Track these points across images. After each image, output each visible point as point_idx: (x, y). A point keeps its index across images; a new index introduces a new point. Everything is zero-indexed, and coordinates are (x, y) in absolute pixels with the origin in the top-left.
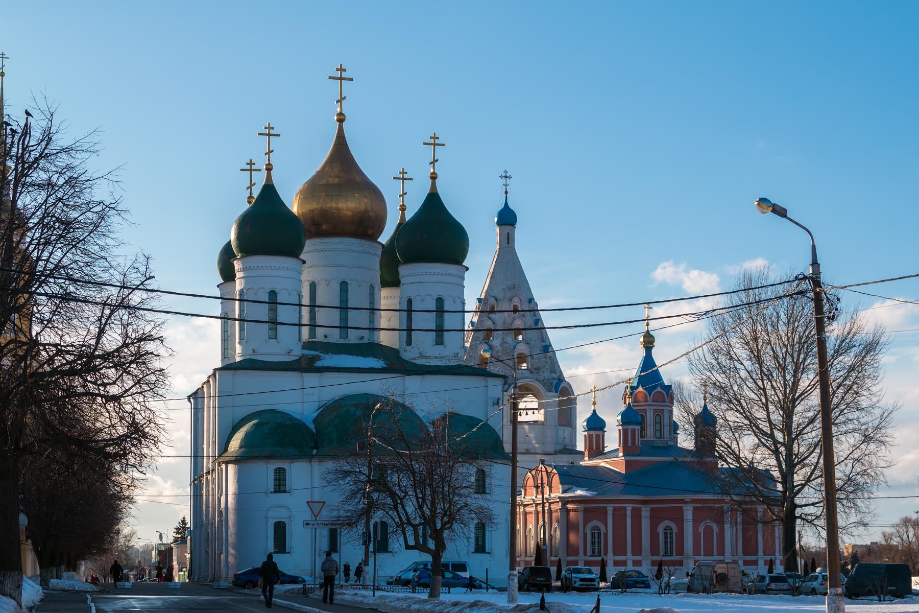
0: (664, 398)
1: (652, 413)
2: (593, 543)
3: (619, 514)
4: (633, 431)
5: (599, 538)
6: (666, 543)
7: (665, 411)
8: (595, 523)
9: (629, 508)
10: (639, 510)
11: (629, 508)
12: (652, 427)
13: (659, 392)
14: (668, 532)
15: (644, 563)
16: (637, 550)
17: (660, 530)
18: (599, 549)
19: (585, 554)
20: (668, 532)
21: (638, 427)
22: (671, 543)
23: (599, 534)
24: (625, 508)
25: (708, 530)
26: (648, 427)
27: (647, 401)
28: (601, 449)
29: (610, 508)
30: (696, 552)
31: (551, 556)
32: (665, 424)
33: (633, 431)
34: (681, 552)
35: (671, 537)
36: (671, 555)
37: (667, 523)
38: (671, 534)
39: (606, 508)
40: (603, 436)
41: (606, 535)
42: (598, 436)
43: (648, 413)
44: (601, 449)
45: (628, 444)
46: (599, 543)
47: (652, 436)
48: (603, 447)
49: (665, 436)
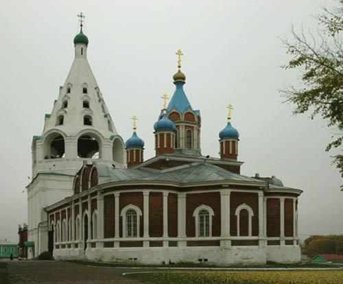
0: (194, 118)
2: (129, 226)
3: (156, 199)
4: (168, 135)
5: (135, 221)
6: (201, 225)
8: (131, 207)
9: (166, 193)
10: (176, 196)
11: (166, 193)
13: (189, 113)
14: (205, 216)
15: (179, 243)
16: (173, 232)
17: (196, 214)
18: (135, 230)
19: (121, 236)
20: (205, 216)
21: (172, 133)
22: (208, 225)
23: (135, 217)
24: (161, 194)
25: (244, 212)
26: (181, 140)
29: (146, 192)
30: (233, 233)
31: (92, 238)
33: (168, 135)
34: (217, 232)
35: (208, 220)
37: (203, 207)
38: (208, 217)
39: (142, 193)
40: (142, 152)
41: (142, 218)
42: (137, 151)
43: (180, 129)
45: (163, 145)
46: (135, 225)
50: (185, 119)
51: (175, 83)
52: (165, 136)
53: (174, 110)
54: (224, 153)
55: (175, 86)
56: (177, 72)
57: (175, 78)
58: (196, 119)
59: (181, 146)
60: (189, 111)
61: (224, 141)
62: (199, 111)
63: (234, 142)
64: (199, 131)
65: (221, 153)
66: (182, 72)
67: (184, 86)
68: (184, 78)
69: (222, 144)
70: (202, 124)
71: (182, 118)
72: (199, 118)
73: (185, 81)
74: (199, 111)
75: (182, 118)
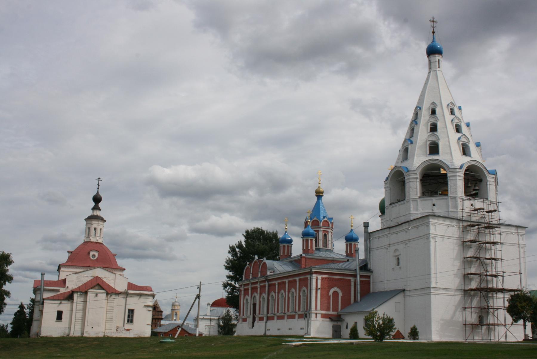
1: (322, 233)
7: (329, 232)
13: (325, 221)
26: (320, 241)
28: (290, 254)
36: (330, 311)
40: (291, 247)
42: (288, 246)
43: (320, 233)
44: (290, 254)
47: (322, 246)
48: (291, 254)
51: (317, 196)
54: (349, 253)
55: (316, 198)
58: (330, 225)
59: (320, 246)
60: (326, 219)
61: (348, 243)
63: (355, 245)
65: (347, 251)
67: (323, 198)
68: (322, 193)
69: (347, 245)
75: (321, 224)
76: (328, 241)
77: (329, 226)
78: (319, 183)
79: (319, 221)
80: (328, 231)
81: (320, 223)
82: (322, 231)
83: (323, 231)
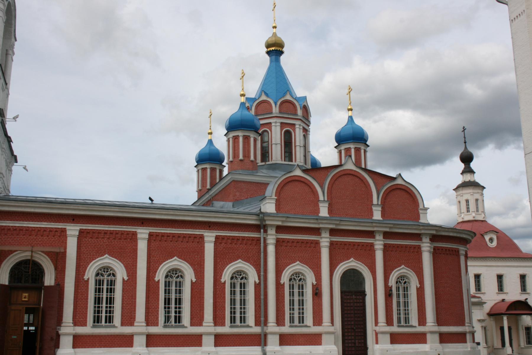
1: (278, 128)
7: (297, 126)
12: (279, 146)
27: (271, 113)
32: (297, 144)
43: (273, 128)
49: (298, 160)
50: (280, 112)
51: (268, 53)
52: (241, 139)
53: (264, 98)
55: (267, 57)
56: (271, 35)
57: (268, 45)
58: (300, 112)
60: (288, 97)
61: (343, 147)
62: (305, 98)
64: (306, 131)
66: (279, 35)
67: (282, 58)
68: (281, 45)
70: (312, 119)
71: (275, 110)
72: (306, 109)
73: (284, 50)
74: (305, 98)
75: (275, 110)
76: (295, 146)
77: (296, 114)
78: (275, 27)
79: (272, 102)
80: (294, 125)
81: (273, 105)
82: (279, 124)
83: (282, 123)
